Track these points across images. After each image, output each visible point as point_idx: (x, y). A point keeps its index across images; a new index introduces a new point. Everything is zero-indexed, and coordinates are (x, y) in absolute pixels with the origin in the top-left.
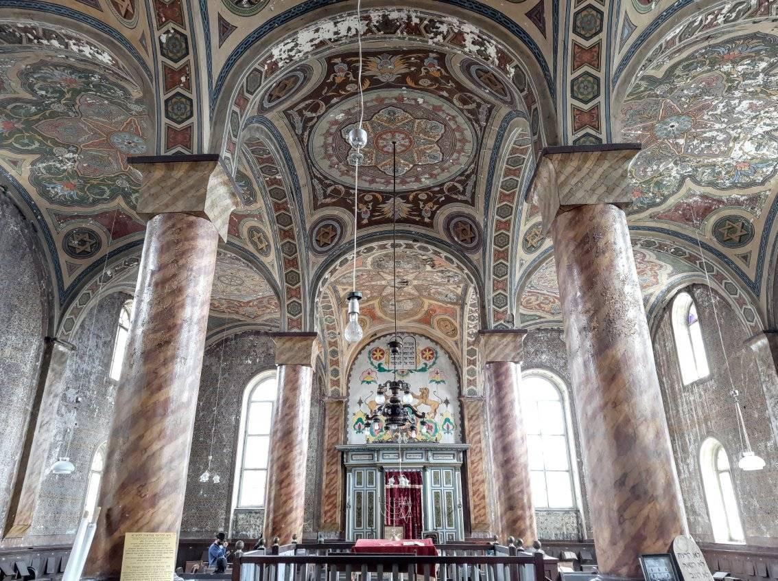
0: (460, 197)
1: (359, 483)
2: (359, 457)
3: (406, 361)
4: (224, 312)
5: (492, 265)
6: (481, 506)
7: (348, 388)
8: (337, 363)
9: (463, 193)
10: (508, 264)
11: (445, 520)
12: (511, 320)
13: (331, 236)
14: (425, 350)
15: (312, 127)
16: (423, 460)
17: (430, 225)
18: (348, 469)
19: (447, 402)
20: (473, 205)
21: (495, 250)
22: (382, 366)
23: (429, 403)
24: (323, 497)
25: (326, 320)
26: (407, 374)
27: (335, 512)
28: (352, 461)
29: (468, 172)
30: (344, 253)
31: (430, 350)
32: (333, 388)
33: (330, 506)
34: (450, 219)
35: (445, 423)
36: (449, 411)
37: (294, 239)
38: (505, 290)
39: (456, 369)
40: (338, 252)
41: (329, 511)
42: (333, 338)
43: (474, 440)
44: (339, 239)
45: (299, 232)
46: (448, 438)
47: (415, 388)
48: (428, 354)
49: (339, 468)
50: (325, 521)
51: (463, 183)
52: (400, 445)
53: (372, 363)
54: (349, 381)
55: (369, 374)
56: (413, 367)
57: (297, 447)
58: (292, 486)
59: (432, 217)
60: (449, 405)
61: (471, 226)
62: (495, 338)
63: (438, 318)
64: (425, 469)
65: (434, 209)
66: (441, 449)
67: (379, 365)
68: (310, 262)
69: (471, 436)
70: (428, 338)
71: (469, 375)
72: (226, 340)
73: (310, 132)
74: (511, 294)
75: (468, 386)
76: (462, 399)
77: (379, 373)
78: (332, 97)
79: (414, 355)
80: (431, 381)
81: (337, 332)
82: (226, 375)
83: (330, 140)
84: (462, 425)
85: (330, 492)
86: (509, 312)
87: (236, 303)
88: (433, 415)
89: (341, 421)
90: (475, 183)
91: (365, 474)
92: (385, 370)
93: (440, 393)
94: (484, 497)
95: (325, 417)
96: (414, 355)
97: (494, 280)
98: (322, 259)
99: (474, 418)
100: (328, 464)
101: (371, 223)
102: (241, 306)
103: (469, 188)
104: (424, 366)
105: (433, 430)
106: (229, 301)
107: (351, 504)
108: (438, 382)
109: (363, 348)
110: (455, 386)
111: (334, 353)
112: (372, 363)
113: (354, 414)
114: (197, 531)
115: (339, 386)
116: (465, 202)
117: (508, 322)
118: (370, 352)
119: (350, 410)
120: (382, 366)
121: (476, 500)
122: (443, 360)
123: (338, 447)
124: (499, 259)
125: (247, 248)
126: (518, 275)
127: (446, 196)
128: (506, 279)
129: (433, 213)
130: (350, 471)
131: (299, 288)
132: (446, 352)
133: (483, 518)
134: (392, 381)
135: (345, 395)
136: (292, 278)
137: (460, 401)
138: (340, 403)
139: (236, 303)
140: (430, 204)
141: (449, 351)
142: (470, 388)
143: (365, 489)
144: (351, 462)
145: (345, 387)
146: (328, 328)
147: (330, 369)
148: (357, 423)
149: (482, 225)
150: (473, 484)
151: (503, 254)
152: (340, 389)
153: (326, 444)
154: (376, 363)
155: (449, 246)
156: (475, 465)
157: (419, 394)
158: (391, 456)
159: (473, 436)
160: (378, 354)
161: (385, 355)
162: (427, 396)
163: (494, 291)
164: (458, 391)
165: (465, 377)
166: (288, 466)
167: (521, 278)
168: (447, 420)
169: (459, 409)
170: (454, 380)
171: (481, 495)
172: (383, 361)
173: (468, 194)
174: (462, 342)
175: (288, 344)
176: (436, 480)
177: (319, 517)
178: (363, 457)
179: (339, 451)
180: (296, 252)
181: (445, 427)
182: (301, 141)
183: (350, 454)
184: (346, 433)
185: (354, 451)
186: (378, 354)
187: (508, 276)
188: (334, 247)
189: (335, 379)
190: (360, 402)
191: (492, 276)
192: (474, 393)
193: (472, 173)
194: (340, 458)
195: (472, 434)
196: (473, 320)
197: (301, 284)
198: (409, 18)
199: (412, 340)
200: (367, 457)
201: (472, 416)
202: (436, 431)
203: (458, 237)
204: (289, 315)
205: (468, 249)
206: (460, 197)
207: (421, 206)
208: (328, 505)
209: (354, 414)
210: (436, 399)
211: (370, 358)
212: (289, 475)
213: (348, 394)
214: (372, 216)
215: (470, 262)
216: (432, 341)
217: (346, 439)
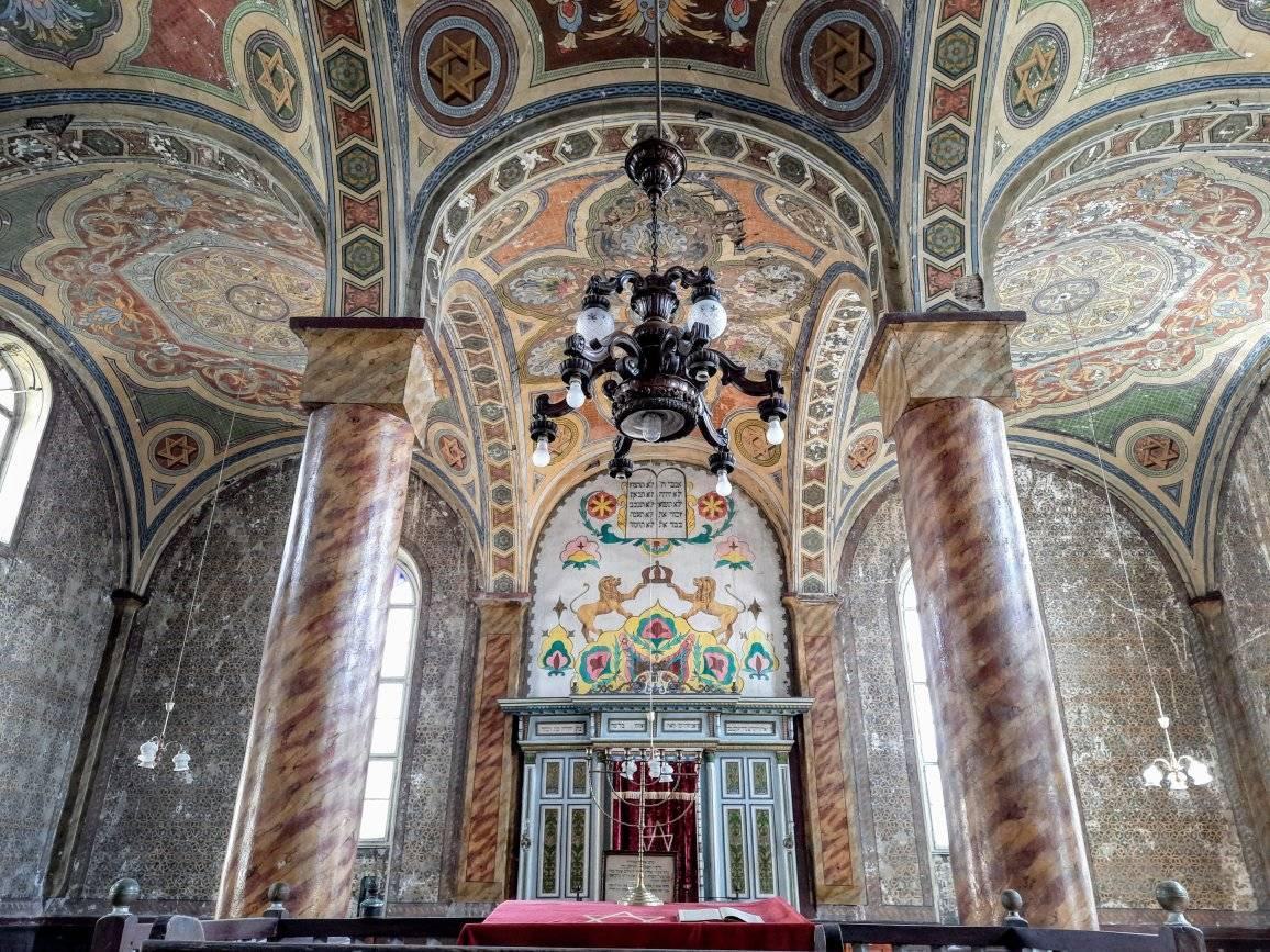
1: (552, 787)
2: (552, 729)
4: (254, 401)
5: (925, 134)
6: (839, 844)
7: (533, 576)
8: (508, 517)
10: (970, 131)
11: (752, 877)
12: (974, 292)
13: (474, 74)
14: (707, 498)
16: (703, 736)
17: (742, 59)
18: (528, 754)
19: (756, 609)
21: (936, 85)
22: (610, 530)
23: (716, 609)
24: (466, 822)
25: (483, 410)
26: (667, 547)
27: (493, 856)
28: (532, 738)
30: (511, 140)
32: (500, 575)
33: (483, 841)
35: (751, 654)
36: (764, 629)
37: (358, 40)
38: (958, 210)
39: (777, 538)
40: (493, 136)
41: (480, 853)
42: (499, 459)
43: (820, 692)
44: (498, 92)
45: (372, 14)
46: (763, 687)
47: (685, 579)
49: (507, 751)
50: (469, 879)
52: (651, 698)
53: (588, 524)
54: (535, 562)
55: (581, 546)
56: (679, 533)
57: (346, 630)
58: (324, 742)
62: (934, 336)
63: (737, 420)
64: (707, 756)
66: (745, 710)
67: (605, 528)
68: (416, 148)
69: (812, 682)
71: (806, 546)
72: (264, 472)
74: (974, 221)
75: (804, 573)
76: (791, 600)
79: (682, 508)
80: (721, 563)
81: (509, 444)
82: (259, 546)
84: (792, 660)
85: (483, 808)
86: (969, 271)
87: (280, 377)
88: (723, 636)
89: (515, 647)
91: (567, 764)
93: (744, 586)
94: (845, 823)
95: (477, 639)
96: (682, 508)
97: (928, 178)
98: (449, 144)
99: (819, 643)
100: (481, 743)
101: (590, 53)
102: (293, 387)
104: (704, 531)
105: (725, 669)
106: (265, 371)
107: (531, 837)
108: (735, 566)
109: (570, 492)
110: (776, 573)
111: (503, 494)
112: (588, 524)
113: (545, 634)
114: (161, 900)
115: (512, 571)
117: (967, 297)
118: (584, 501)
119: (536, 625)
120: (610, 530)
121: (828, 829)
122: (746, 517)
123: (504, 703)
124: (942, 116)
125: (247, 117)
126: (989, 181)
128: (963, 178)
130: (532, 761)
131: (377, 198)
132: (755, 503)
133: (844, 872)
134: (645, 272)
135: (525, 588)
136: (357, 169)
137: (786, 606)
138: (513, 606)
139: (280, 377)
141: (760, 498)
142: (808, 576)
143: (565, 802)
144: (534, 739)
145: (525, 573)
146: (489, 434)
147: (493, 531)
148: (550, 653)
150: (820, 793)
151: (956, 102)
153: (478, 698)
154: (597, 524)
155: (793, 121)
156: (824, 747)
157: (692, 590)
158: (629, 725)
159: (817, 684)
160: (602, 506)
161: (618, 508)
162: (710, 595)
163: (928, 211)
164: (780, 584)
165: (798, 552)
166: (313, 684)
167: (994, 194)
168: (757, 647)
169: (784, 624)
170: (772, 560)
171: (839, 819)
172: (612, 520)
174: (791, 473)
175: (342, 351)
177: (454, 868)
178: (562, 729)
179: (508, 712)
180: (367, 85)
181: (752, 663)
183: (532, 720)
184: (526, 674)
185: (540, 712)
186: (602, 506)
187: (968, 168)
188: (482, 113)
189: (504, 554)
190: (560, 608)
191: (924, 167)
192: (819, 587)
194: (509, 731)
195: (815, 677)
196: (819, 416)
197: (381, 186)
199: (678, 478)
200: (572, 728)
201: (814, 640)
202: (732, 669)
204: (348, 275)
208: (477, 840)
209: (545, 634)
210: (731, 602)
211: (583, 514)
212: (314, 707)
213: (533, 590)
214: (588, 26)
215: (853, 156)
217: (524, 690)
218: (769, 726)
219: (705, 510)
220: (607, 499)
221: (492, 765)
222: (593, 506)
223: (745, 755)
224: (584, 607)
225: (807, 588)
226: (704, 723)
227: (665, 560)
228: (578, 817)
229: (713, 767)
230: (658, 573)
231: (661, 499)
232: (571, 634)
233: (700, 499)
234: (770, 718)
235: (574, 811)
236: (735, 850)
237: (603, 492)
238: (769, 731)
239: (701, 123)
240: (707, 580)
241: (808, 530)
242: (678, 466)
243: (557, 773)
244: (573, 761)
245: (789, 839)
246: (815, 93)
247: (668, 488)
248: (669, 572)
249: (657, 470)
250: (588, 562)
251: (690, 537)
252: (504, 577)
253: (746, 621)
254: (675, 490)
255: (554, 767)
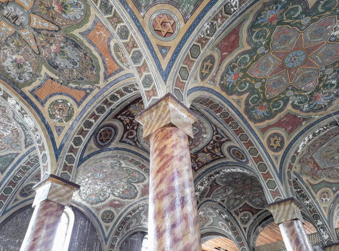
0: (125, 135)
9: (127, 137)
15: (214, 131)
20: (120, 141)
29: (137, 143)
34: (115, 128)
51: (133, 139)
59: (120, 119)
61: (109, 139)
65: (124, 122)
73: (213, 129)
78: (214, 143)
83: (201, 126)
90: (131, 144)
103: (129, 141)
116: (122, 138)
127: (129, 130)
129: (122, 121)
140: (128, 121)
149: (110, 147)
173: (127, 140)
182: (215, 126)
193: (136, 145)
198: (214, 177)
203: (103, 131)
205: (96, 138)
206: (125, 135)
207: (130, 118)
239: (110, 109)
246: (102, 130)
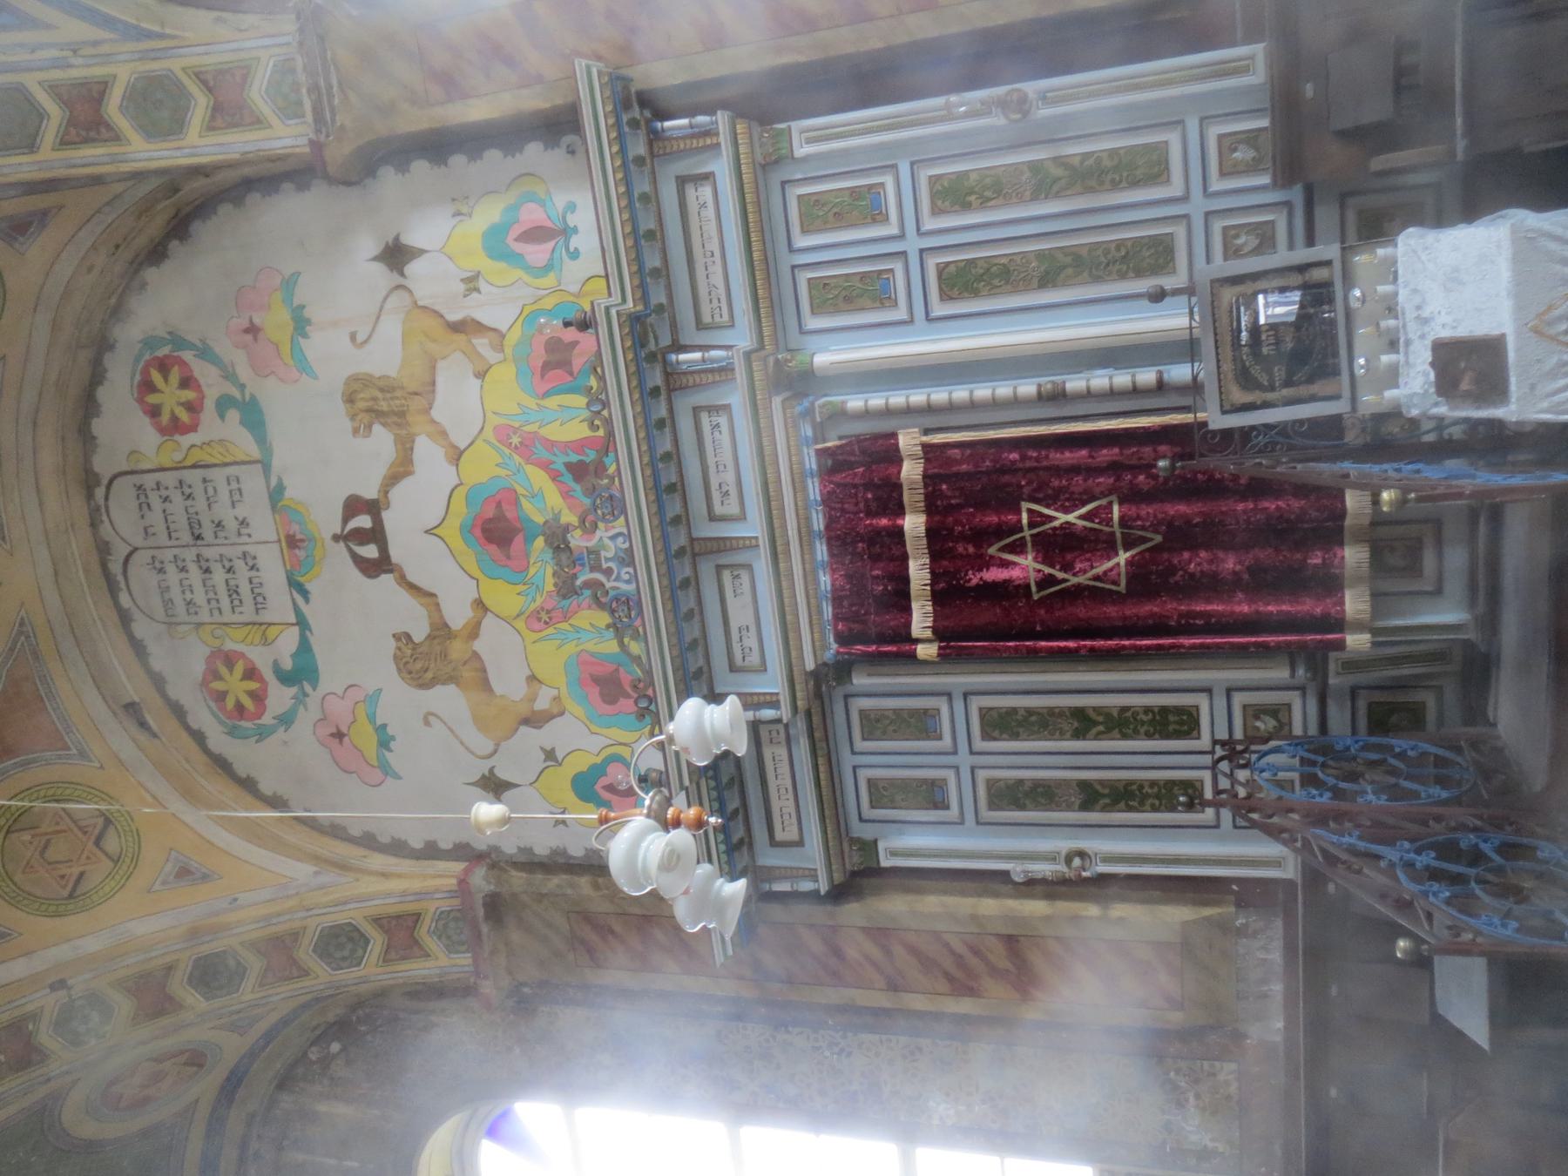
1: (932, 795)
2: (782, 804)
3: (231, 525)
7: (431, 851)
14: (154, 412)
16: (735, 397)
18: (854, 860)
19: (396, 255)
22: (287, 664)
31: (148, 387)
47: (362, 462)
48: (170, 397)
53: (286, 720)
54: (398, 848)
55: (339, 735)
60: (412, 239)
64: (799, 382)
67: (286, 678)
70: (88, 405)
71: (177, 126)
75: (258, 122)
77: (325, 685)
79: (192, 477)
80: (304, 367)
88: (482, 343)
92: (304, 647)
104: (233, 415)
107: (1063, 844)
108: (301, 324)
112: (286, 720)
115: (417, 917)
120: (287, 664)
122: (170, 302)
130: (870, 847)
138: (496, 907)
144: (813, 853)
147: (322, 975)
152: (431, 907)
157: (382, 441)
158: (740, 614)
161: (230, 646)
162: (387, 387)
168: (495, 244)
172: (261, 658)
176: (861, 292)
181: (537, 253)
186: (237, 687)
210: (391, 328)
211: (262, 734)
216: (97, 376)
218: (691, 192)
219: (184, 416)
220: (217, 676)
221: (887, 952)
222: (240, 708)
223: (786, 260)
224: (481, 723)
225: (290, 110)
226: (701, 398)
227: (326, 519)
228: (1000, 724)
229: (827, 357)
230: (361, 536)
231: (186, 537)
232: (550, 755)
233: (163, 431)
234: (668, 192)
235: (986, 736)
236: (1052, 271)
237: (204, 683)
238: (706, 192)
240: (350, 399)
241: (123, 124)
242: (100, 492)
243: (893, 783)
244: (860, 745)
245: (1003, 104)
247: (155, 518)
248: (354, 506)
249: (121, 550)
250: (372, 718)
251: (254, 452)
252: (441, 933)
253: (431, 279)
254: (154, 499)
255: (882, 793)
